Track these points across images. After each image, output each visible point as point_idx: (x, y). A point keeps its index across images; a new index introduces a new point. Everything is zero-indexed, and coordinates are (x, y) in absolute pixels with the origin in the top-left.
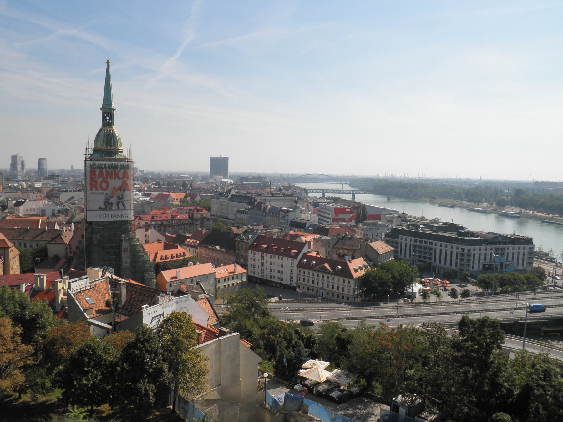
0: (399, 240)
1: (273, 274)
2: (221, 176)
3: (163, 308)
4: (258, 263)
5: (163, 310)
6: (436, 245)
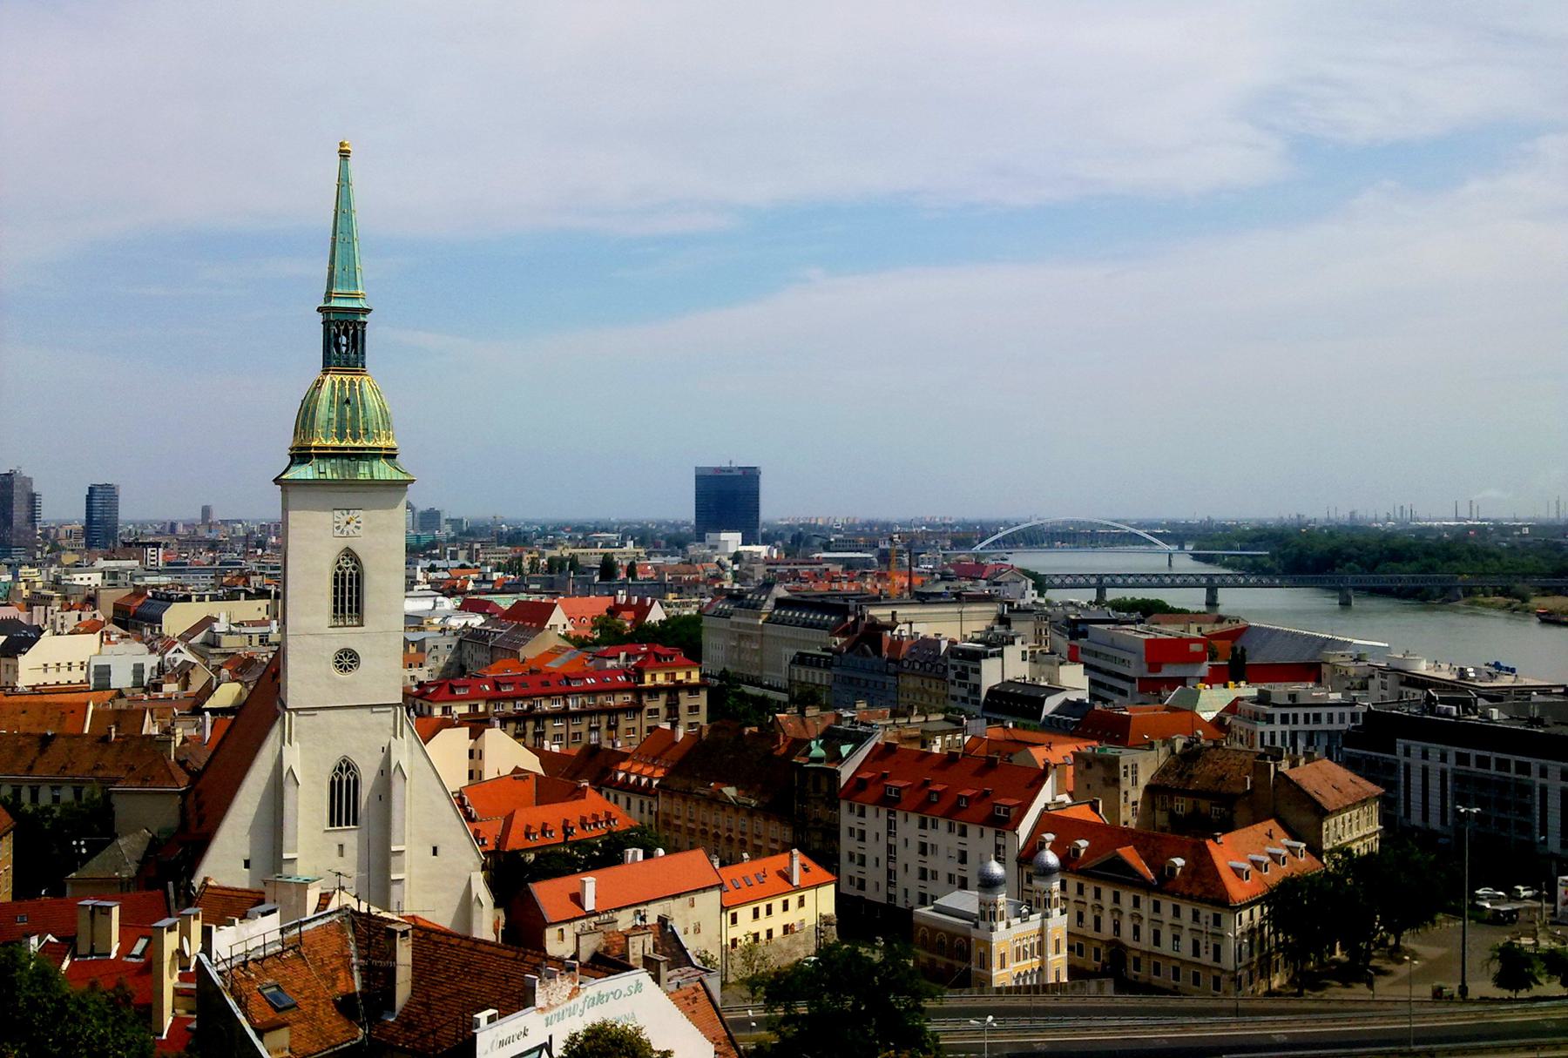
2: (738, 536)
3: (548, 1023)
4: (874, 849)
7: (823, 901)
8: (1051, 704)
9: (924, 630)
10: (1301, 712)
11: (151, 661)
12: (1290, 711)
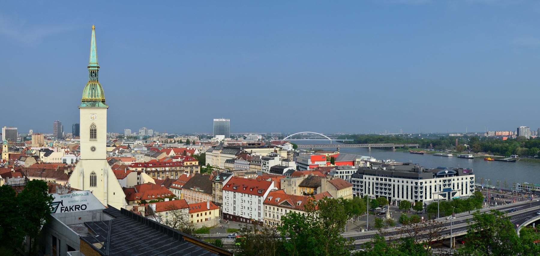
0: (364, 180)
1: (244, 211)
2: (224, 136)
4: (231, 202)
5: (62, 199)
6: (394, 181)
7: (216, 213)
8: (285, 170)
9: (258, 154)
10: (345, 171)
11: (75, 158)
12: (342, 171)
